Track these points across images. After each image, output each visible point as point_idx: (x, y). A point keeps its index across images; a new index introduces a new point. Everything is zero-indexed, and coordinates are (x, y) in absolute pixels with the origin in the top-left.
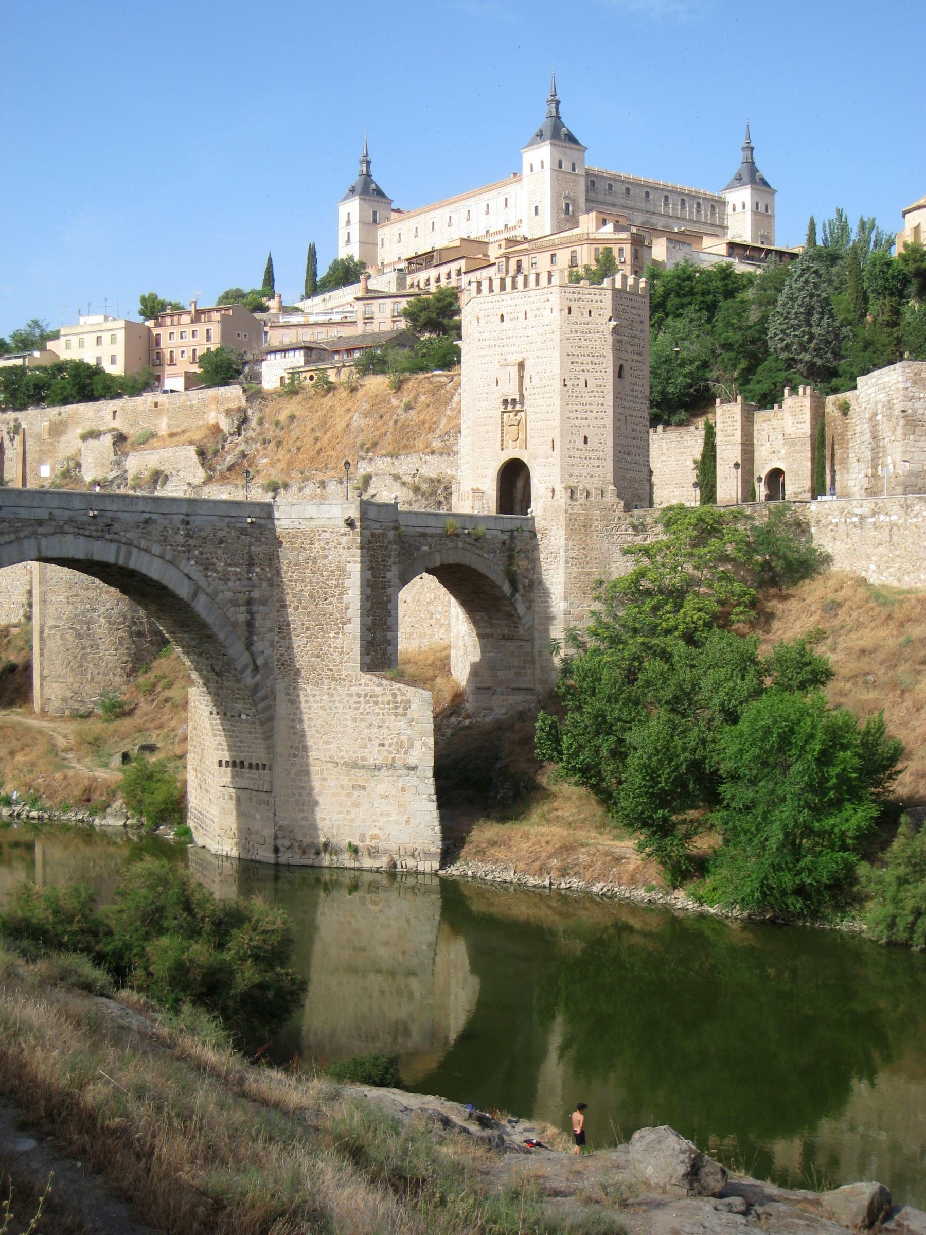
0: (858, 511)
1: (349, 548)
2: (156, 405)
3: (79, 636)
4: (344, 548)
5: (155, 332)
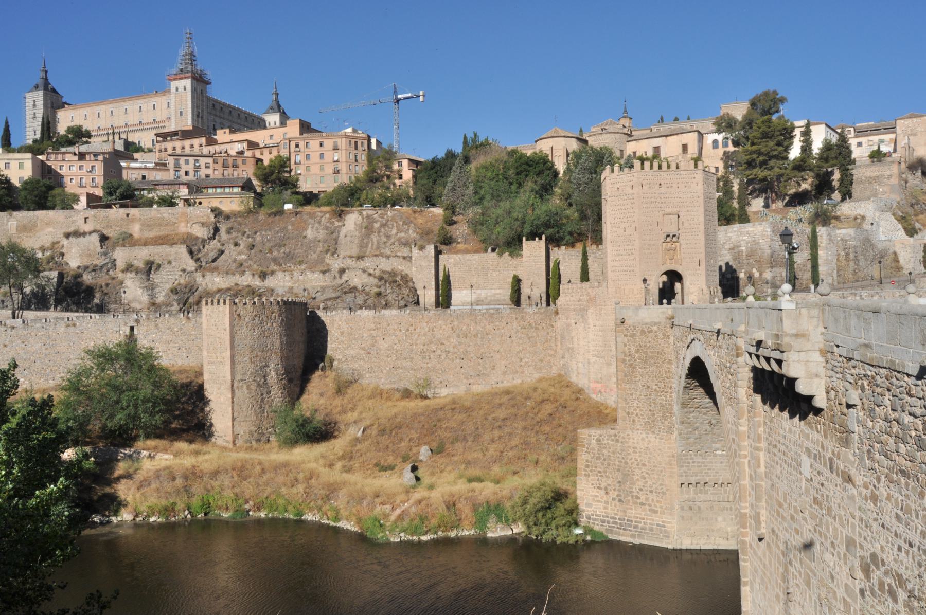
2: (128, 215)
3: (259, 385)
5: (49, 163)
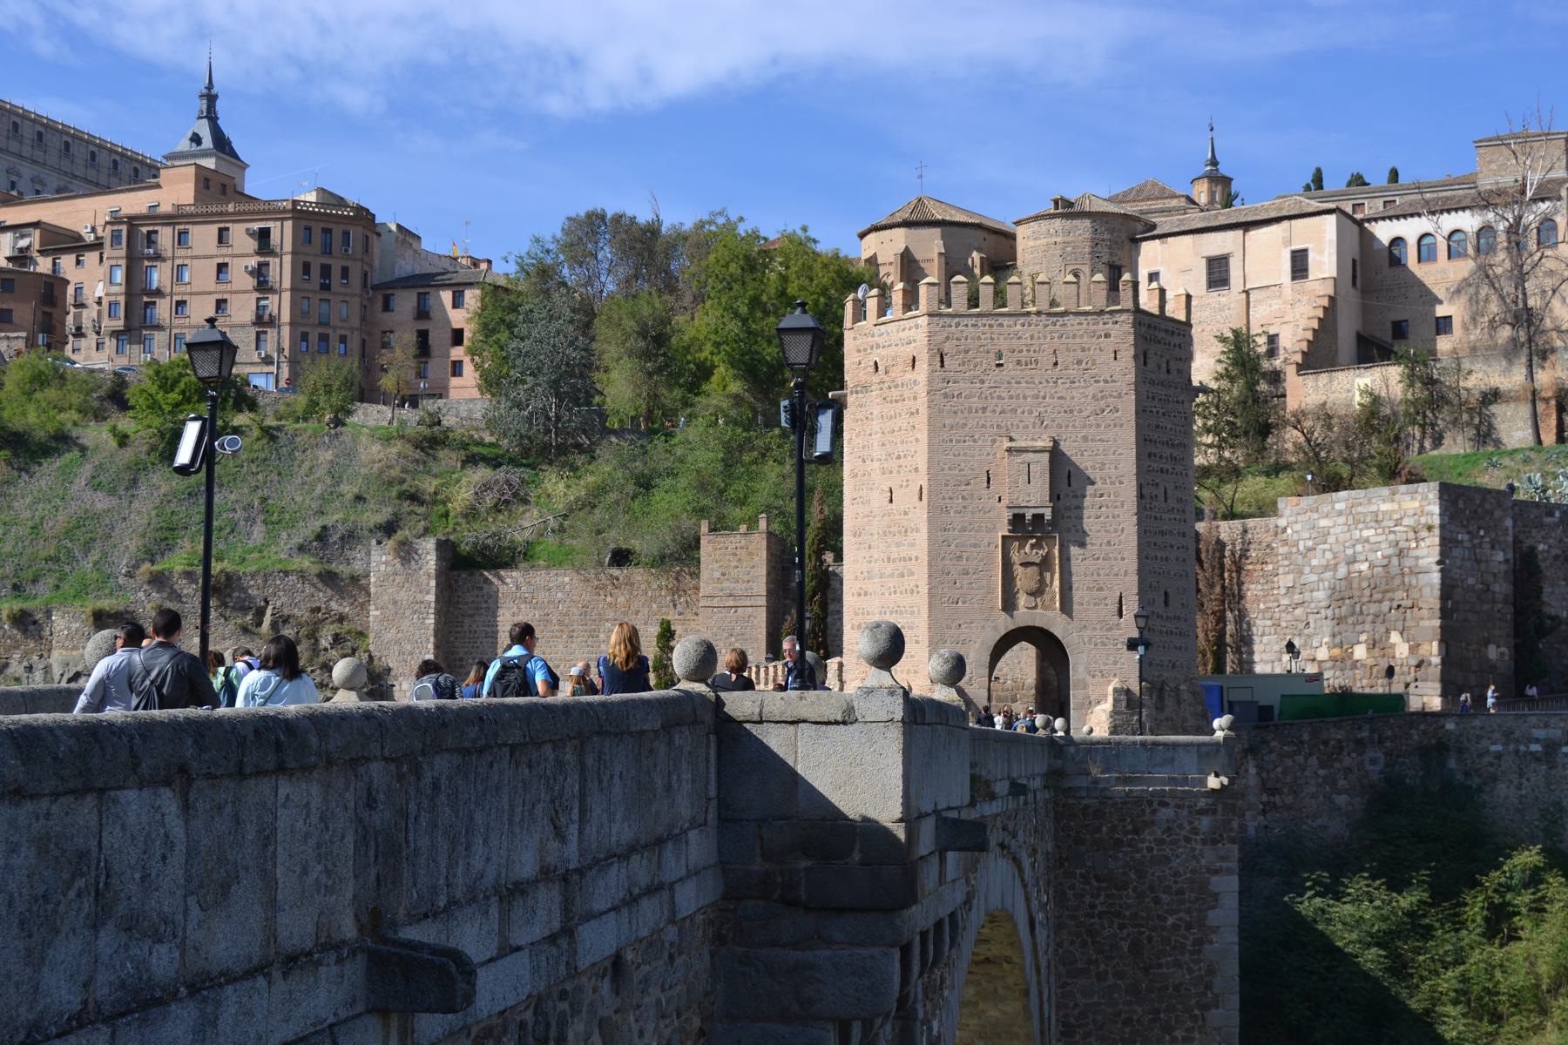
0: (1540, 733)
1: (1214, 842)
4: (1204, 842)
